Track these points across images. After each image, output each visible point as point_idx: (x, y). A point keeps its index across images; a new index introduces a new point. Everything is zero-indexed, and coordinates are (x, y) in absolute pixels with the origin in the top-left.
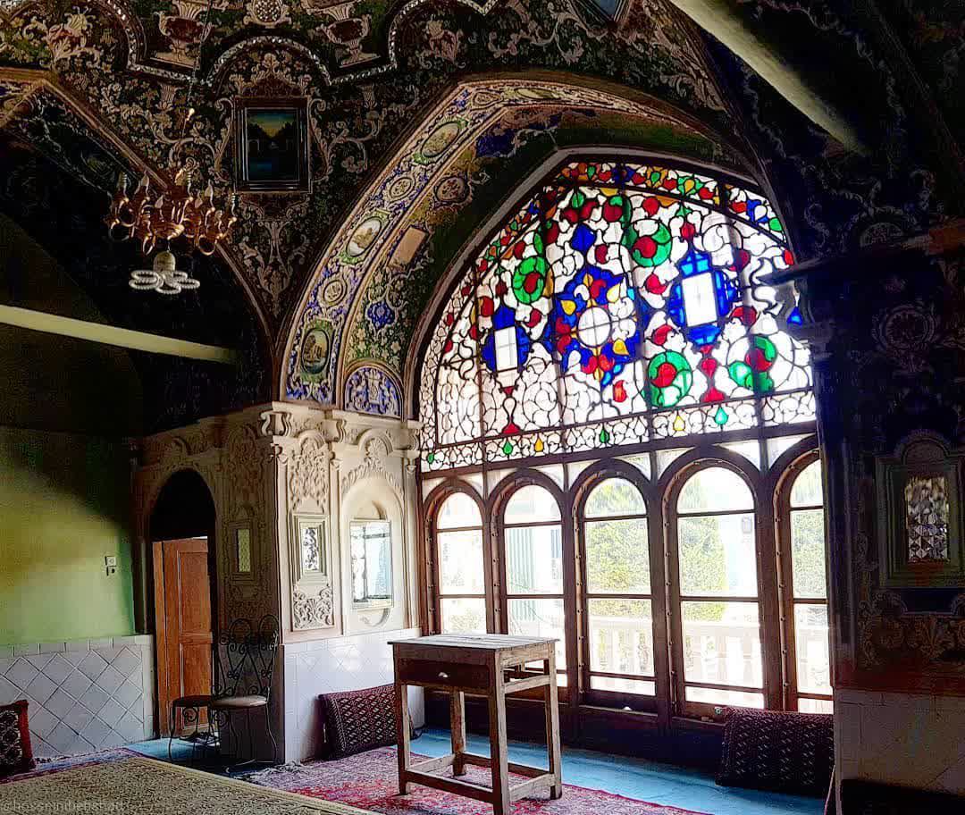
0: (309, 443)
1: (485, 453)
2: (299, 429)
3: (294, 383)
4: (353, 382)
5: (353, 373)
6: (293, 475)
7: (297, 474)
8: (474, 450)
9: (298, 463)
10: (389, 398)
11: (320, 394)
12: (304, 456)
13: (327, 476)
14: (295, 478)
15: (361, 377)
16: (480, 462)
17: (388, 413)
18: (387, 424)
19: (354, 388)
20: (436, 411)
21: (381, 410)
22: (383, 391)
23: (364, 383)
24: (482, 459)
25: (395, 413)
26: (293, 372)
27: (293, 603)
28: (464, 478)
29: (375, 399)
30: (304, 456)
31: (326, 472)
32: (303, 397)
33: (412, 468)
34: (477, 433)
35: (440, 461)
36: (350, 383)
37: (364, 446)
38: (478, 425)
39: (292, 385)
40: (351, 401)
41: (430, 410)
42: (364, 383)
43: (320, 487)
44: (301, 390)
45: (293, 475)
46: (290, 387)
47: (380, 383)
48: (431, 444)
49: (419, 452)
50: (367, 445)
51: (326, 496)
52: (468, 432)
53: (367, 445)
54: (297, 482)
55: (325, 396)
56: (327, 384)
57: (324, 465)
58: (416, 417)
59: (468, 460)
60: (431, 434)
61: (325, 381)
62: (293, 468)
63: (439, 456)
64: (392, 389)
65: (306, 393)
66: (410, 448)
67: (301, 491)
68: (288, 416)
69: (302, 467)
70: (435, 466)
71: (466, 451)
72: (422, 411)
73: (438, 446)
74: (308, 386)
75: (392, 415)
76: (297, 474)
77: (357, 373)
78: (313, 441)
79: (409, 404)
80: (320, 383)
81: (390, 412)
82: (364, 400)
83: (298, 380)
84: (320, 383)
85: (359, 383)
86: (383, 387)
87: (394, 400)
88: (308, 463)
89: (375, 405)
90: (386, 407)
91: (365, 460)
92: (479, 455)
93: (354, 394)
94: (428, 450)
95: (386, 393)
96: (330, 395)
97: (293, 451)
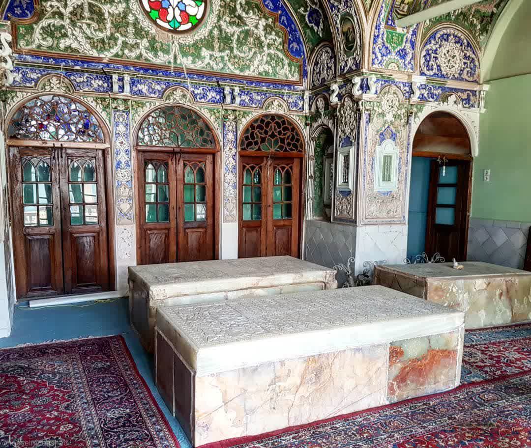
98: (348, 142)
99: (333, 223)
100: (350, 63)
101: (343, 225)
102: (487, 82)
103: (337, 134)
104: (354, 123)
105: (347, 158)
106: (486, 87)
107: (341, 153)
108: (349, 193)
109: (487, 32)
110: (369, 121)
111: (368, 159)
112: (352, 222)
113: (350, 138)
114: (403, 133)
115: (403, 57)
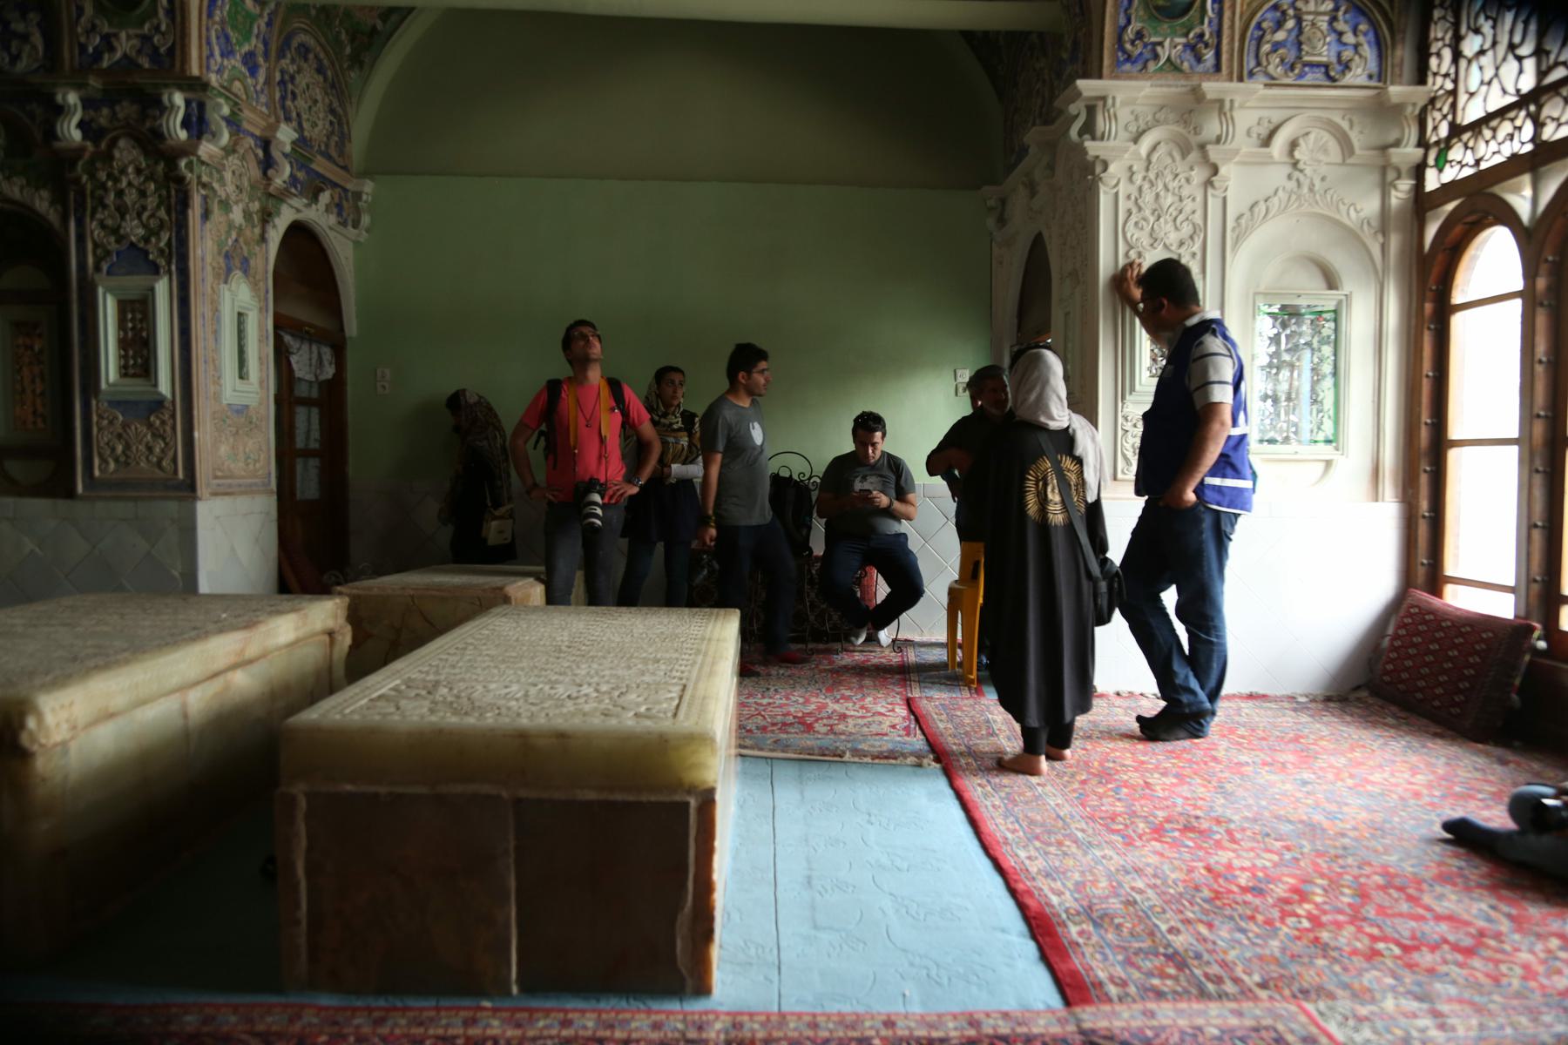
0: (1162, 150)
1: (1539, 125)
2: (1143, 127)
3: (1133, 43)
4: (1265, 25)
5: (1266, 7)
6: (1130, 213)
7: (1140, 209)
8: (1518, 123)
9: (1140, 189)
10: (1356, 47)
11: (1188, 55)
12: (1152, 175)
13: (1199, 213)
14: (1133, 219)
15: (1284, 13)
16: (1529, 147)
17: (1348, 79)
18: (1346, 99)
19: (1268, 37)
20: (1457, 56)
21: (1330, 74)
22: (1341, 34)
23: (1290, 24)
24: (1532, 140)
25: (1370, 77)
26: (1129, 22)
27: (1120, 433)
28: (1497, 190)
29: (1324, 52)
30: (1152, 175)
31: (1199, 199)
32: (1152, 66)
33: (1406, 185)
34: (1528, 83)
35: (1459, 165)
36: (1259, 26)
37: (1286, 148)
38: (1530, 65)
39: (1128, 46)
40: (1259, 64)
41: (1447, 54)
42: (1290, 24)
43: (1186, 229)
44: (1147, 55)
45: (1130, 213)
46: (1124, 51)
47: (1334, 19)
48: (1444, 131)
49: (1421, 151)
50: (1293, 145)
51: (1197, 247)
52: (1511, 90)
53: (1293, 145)
54: (1136, 224)
55: (1199, 59)
56: (1202, 35)
57: (1194, 189)
58: (1421, 76)
59: (1507, 150)
60: (1446, 109)
61: (1197, 30)
62: (1129, 197)
63: (1456, 153)
64: (1363, 27)
65: (1156, 57)
66: (1397, 144)
67: (1146, 241)
68: (1110, 102)
69: (1148, 197)
70: (1449, 174)
71: (1506, 128)
72: (1433, 62)
73: (1456, 130)
74: (1161, 44)
75: (1363, 80)
76: (1140, 209)
77: (1275, 7)
78: (1171, 145)
79: (1404, 54)
80: (1186, 35)
81: (1358, 75)
82: (1291, 56)
83: (1139, 35)
84: (1186, 35)
85: (1279, 25)
86: (1340, 26)
87: (1368, 52)
88: (1160, 186)
89: (1318, 65)
90: (1347, 67)
91: (1290, 177)
92: (1528, 130)
93: (1266, 48)
94: (1437, 143)
95: (1349, 38)
96: (1209, 55)
97: (1130, 168)
98: (139, 260)
99: (82, 498)
100: (125, 44)
101: (135, 499)
102: (366, 174)
103: (81, 239)
104: (162, 213)
105: (137, 313)
106: (368, 187)
107: (108, 290)
108: (158, 404)
109: (361, 67)
110: (206, 215)
111: (208, 315)
112: (179, 486)
113: (146, 253)
114: (256, 263)
115: (253, 71)
